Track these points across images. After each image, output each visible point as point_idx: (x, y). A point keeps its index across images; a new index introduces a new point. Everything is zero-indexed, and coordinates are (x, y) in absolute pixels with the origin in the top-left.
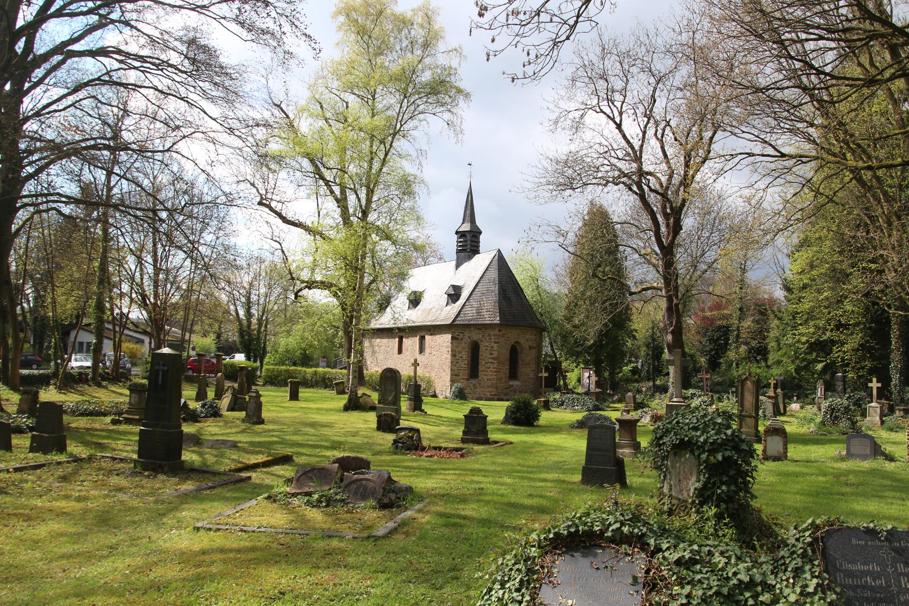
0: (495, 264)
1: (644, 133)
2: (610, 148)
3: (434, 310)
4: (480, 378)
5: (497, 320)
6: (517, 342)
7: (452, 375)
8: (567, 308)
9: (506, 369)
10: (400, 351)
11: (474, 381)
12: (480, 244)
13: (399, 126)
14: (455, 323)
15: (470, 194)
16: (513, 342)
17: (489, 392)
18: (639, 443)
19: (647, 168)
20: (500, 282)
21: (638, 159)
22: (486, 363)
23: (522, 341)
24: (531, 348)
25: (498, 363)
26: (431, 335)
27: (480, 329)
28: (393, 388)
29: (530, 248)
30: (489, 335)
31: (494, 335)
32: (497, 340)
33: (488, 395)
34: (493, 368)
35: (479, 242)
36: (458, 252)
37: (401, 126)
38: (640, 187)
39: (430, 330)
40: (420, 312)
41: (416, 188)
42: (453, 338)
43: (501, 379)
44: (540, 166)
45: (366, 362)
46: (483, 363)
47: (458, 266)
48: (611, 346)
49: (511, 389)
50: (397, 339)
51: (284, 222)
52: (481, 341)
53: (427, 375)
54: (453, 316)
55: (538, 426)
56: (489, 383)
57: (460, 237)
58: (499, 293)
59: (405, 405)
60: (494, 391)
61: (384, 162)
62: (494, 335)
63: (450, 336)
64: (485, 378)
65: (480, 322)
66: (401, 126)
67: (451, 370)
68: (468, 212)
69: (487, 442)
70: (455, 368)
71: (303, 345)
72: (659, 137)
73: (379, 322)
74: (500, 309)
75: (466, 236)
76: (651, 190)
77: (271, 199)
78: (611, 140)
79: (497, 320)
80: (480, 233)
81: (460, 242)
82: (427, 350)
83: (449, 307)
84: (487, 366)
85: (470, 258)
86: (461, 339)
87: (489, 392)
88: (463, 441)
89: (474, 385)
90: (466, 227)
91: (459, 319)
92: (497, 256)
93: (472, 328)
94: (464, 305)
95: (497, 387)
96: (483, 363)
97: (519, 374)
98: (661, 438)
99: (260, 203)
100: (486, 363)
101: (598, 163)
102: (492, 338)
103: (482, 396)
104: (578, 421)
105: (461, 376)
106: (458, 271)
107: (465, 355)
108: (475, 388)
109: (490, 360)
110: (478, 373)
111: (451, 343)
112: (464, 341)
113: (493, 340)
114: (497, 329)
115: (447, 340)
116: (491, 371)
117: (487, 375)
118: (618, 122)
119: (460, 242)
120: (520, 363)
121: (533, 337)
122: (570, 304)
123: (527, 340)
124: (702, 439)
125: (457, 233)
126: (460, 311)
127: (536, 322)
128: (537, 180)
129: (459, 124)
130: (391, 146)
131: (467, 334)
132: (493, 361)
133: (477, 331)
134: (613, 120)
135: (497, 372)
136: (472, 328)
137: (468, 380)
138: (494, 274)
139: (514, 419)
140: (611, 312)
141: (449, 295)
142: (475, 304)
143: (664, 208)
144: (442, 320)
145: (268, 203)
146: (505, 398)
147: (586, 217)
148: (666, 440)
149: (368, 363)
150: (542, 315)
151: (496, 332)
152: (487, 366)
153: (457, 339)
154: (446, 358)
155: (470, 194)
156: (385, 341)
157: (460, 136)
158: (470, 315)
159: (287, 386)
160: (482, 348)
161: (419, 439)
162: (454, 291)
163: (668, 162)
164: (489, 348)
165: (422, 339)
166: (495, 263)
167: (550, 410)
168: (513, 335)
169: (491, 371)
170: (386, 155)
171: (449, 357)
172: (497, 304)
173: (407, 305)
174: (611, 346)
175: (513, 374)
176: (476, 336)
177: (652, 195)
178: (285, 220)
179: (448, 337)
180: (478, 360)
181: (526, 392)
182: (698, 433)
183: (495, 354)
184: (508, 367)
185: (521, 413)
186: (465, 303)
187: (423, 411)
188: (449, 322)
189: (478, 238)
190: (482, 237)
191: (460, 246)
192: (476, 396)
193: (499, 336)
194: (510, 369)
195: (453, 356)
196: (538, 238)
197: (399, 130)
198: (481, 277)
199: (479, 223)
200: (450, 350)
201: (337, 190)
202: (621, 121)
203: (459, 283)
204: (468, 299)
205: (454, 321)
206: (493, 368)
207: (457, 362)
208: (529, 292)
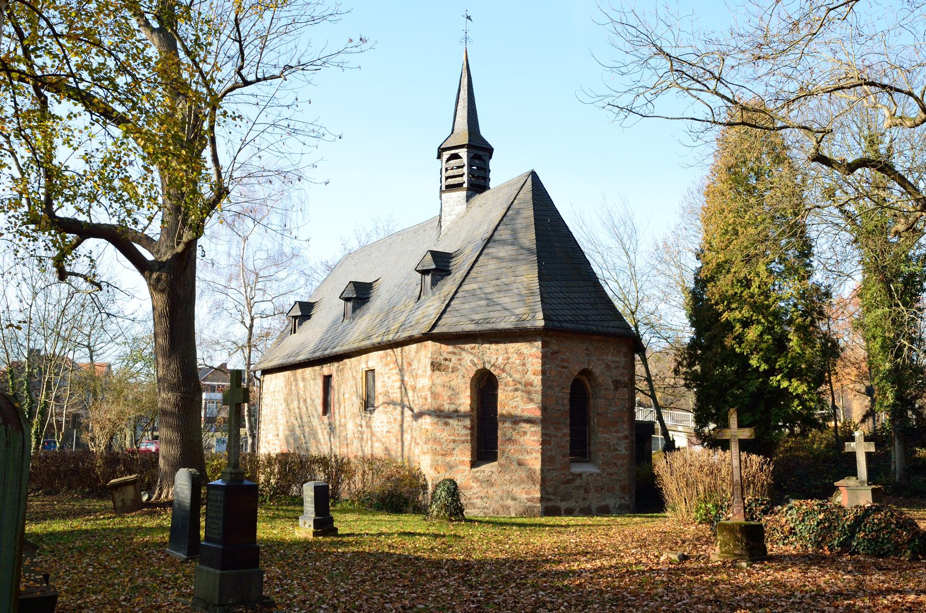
6: (586, 373)
9: (564, 434)
11: (487, 468)
12: (491, 176)
16: (576, 370)
23: (597, 370)
49: (578, 482)
80: (489, 151)
97: (593, 448)
120: (594, 420)
123: (608, 367)
146: (563, 505)
162: (435, 261)
181: (611, 490)
184: (567, 431)
190: (492, 164)
194: (572, 434)
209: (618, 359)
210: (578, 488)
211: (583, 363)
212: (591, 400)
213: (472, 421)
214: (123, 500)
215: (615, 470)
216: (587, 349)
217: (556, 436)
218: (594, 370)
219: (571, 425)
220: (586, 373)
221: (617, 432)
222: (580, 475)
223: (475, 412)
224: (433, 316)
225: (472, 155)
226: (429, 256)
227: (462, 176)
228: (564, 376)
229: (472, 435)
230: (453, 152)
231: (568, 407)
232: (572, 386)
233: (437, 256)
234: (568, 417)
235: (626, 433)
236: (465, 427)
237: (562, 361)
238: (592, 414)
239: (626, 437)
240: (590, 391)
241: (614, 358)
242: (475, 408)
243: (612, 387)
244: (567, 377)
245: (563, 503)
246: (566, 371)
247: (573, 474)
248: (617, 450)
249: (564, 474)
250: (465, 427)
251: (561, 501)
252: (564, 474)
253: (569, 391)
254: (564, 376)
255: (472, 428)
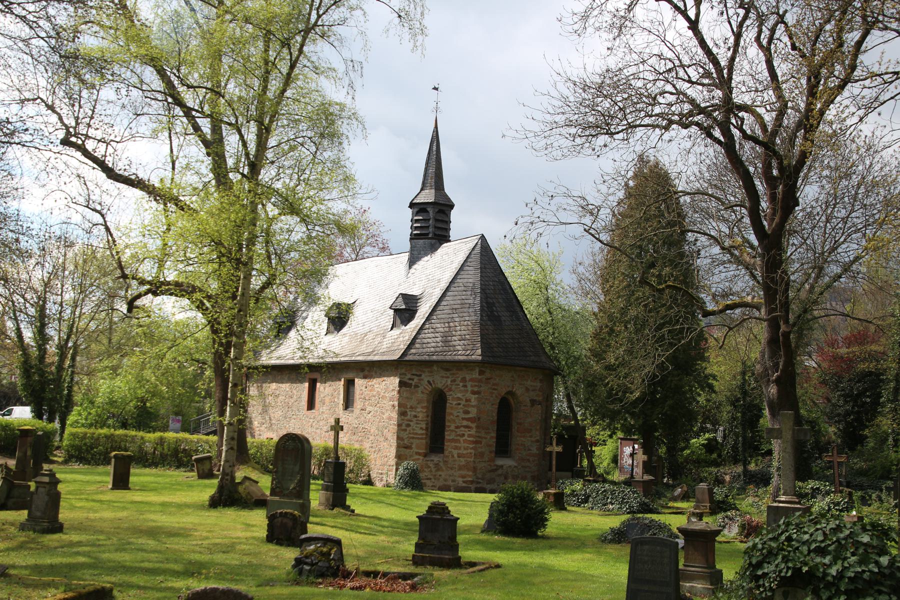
0: (476, 261)
1: (738, 36)
2: (677, 63)
3: (370, 336)
4: (446, 453)
5: (477, 355)
6: (510, 393)
7: (398, 447)
8: (596, 335)
9: (490, 438)
10: (311, 405)
11: (436, 458)
13: (314, 16)
14: (407, 358)
15: (435, 138)
16: (503, 392)
17: (463, 477)
18: (720, 573)
19: (739, 98)
20: (483, 290)
21: (725, 83)
22: (457, 427)
23: (519, 391)
24: (533, 402)
25: (477, 427)
26: (365, 377)
27: (447, 370)
28: (297, 468)
29: (534, 235)
30: (464, 380)
31: (471, 380)
32: (476, 389)
33: (460, 482)
34: (469, 436)
35: (448, 222)
36: (413, 238)
37: (319, 16)
38: (726, 132)
39: (362, 370)
40: (346, 339)
41: (343, 127)
42: (401, 384)
43: (482, 455)
44: (554, 93)
45: (251, 423)
46: (452, 428)
47: (412, 262)
48: (670, 402)
49: (500, 472)
50: (307, 385)
51: (109, 177)
52: (450, 390)
53: (357, 446)
54: (403, 347)
55: (544, 537)
56: (463, 461)
57: (417, 214)
58: (482, 310)
59: (316, 497)
60: (470, 475)
61: (288, 80)
62: (471, 380)
63: (397, 380)
64: (455, 452)
65: (448, 358)
66: (319, 16)
67: (398, 438)
68: (432, 171)
69: (456, 563)
70: (404, 435)
71: (140, 393)
72: (765, 43)
73: (276, 354)
74: (482, 336)
75: (428, 212)
76: (745, 136)
77: (87, 137)
78: (678, 48)
79: (477, 355)
80: (451, 206)
81: (417, 221)
82: (358, 404)
83: (396, 332)
84: (459, 432)
85: (433, 249)
86: (416, 386)
87: (463, 477)
88: (416, 561)
89: (437, 465)
90: (428, 196)
91: (413, 351)
92: (479, 246)
93: (435, 368)
94: (421, 328)
95: (475, 469)
96: (452, 428)
98: (759, 565)
99: (65, 142)
100: (457, 427)
101: (654, 90)
102: (469, 384)
103: (450, 483)
104: (612, 530)
105: (415, 450)
106: (412, 271)
107: (422, 413)
108: (438, 470)
109: (465, 423)
110: (443, 444)
111: (399, 392)
112: (420, 390)
113: (469, 389)
114: (477, 370)
115: (391, 387)
116: (465, 441)
117: (460, 448)
118: (693, 17)
119: (417, 221)
120: (515, 427)
121: (538, 384)
122: (601, 328)
123: (527, 390)
124: (833, 571)
125: (412, 205)
126: (415, 338)
127: (543, 359)
128: (549, 118)
129: (418, 16)
130: (301, 51)
131: (426, 378)
132: (469, 424)
133: (443, 373)
134: (684, 13)
135: (476, 442)
136: (435, 368)
137: (425, 455)
138: (473, 277)
139: (503, 524)
140: (671, 345)
141: (397, 311)
142: (440, 327)
143: (767, 168)
144: (383, 354)
145: (80, 142)
146: (489, 487)
147: (631, 183)
148: (768, 568)
149: (256, 424)
150: (553, 348)
151: (475, 375)
152: (459, 432)
153: (409, 385)
154: (390, 418)
155: (435, 138)
156: (286, 387)
157: (420, 38)
158: (432, 343)
159: (109, 463)
160: (451, 402)
161: (341, 557)
162: (405, 303)
163: (778, 89)
164: (463, 402)
165: (350, 384)
166: (476, 258)
167: (565, 509)
168: (504, 382)
169: (465, 441)
170: (292, 67)
171: (395, 415)
172: (477, 328)
173: (325, 326)
174: (670, 402)
175: (503, 448)
176: (441, 381)
177: (748, 145)
178: (111, 174)
179: (392, 383)
180: (444, 421)
181: (524, 478)
182: (827, 560)
183: (473, 412)
184: (494, 435)
185: (515, 514)
186: (424, 324)
187: (347, 508)
188: (396, 357)
189: (448, 216)
190: (454, 215)
191: (416, 228)
192: (441, 483)
193: (480, 381)
194: (498, 438)
195: (402, 414)
196: (550, 217)
197: (315, 24)
198: (452, 282)
199: (449, 189)
200: (396, 403)
201: (205, 125)
202: (698, 15)
203: (415, 292)
204: (428, 319)
205: (404, 354)
206: (469, 436)
207: (408, 425)
208: (532, 308)
209: (535, 384)
210: (500, 475)
211: (508, 387)
212: (514, 413)
213: (427, 424)
214: (203, 469)
215: (528, 464)
216: (513, 377)
217: (486, 438)
218: (517, 392)
219: (497, 431)
220: (510, 393)
221: (531, 437)
222: (502, 466)
223: (429, 418)
224: (402, 346)
225: (437, 210)
226: (400, 299)
227: (428, 227)
228: (494, 395)
229: (427, 434)
230: (422, 206)
231: (496, 418)
232: (500, 403)
233: (407, 298)
234: (496, 425)
235: (538, 438)
236: (421, 428)
237: (494, 385)
238: (514, 423)
239: (537, 441)
240: (514, 406)
241: (532, 383)
242: (430, 414)
243: (529, 404)
244: (496, 396)
245: (489, 486)
246: (495, 392)
247: (497, 466)
248: (529, 450)
249: (490, 465)
250: (421, 428)
251: (487, 484)
252: (490, 465)
253: (497, 407)
254: (494, 395)
255: (427, 429)
